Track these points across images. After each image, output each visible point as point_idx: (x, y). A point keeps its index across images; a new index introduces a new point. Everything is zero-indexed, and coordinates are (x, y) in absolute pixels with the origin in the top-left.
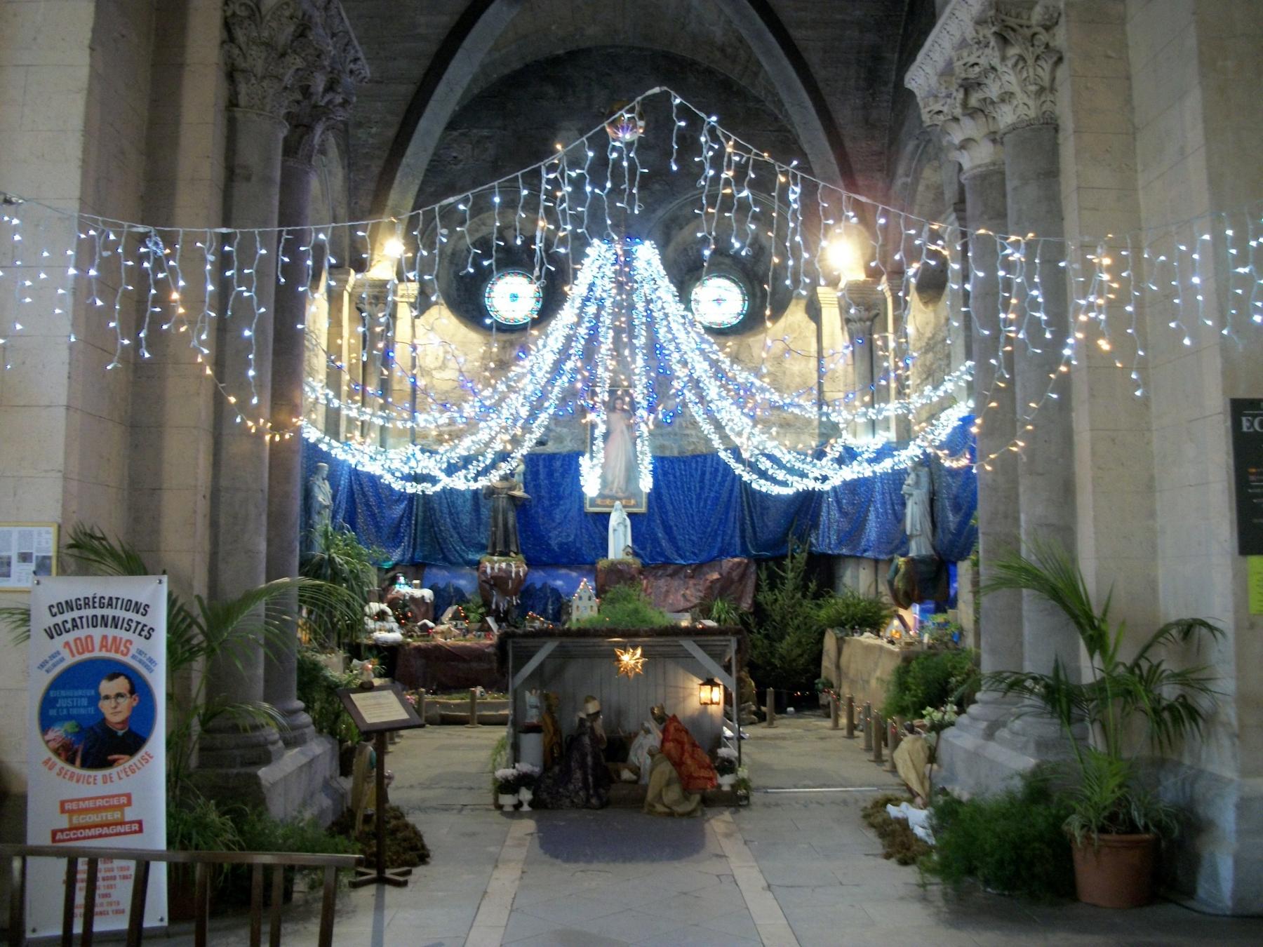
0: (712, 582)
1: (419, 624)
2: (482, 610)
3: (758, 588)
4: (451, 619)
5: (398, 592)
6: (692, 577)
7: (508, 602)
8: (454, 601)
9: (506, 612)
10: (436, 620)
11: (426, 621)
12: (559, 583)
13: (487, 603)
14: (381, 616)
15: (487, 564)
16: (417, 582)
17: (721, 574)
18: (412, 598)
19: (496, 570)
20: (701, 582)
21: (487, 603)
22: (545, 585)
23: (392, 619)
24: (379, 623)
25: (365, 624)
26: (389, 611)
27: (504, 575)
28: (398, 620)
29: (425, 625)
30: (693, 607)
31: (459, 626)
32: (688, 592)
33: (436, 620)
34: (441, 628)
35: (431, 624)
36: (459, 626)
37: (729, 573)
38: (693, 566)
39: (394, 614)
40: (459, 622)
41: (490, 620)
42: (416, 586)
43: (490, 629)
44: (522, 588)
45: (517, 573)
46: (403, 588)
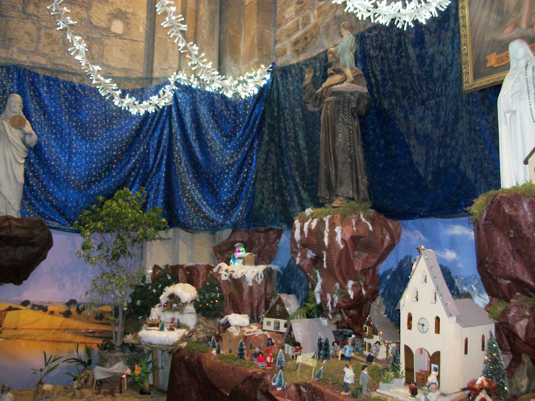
31: (283, 329)
40: (282, 322)
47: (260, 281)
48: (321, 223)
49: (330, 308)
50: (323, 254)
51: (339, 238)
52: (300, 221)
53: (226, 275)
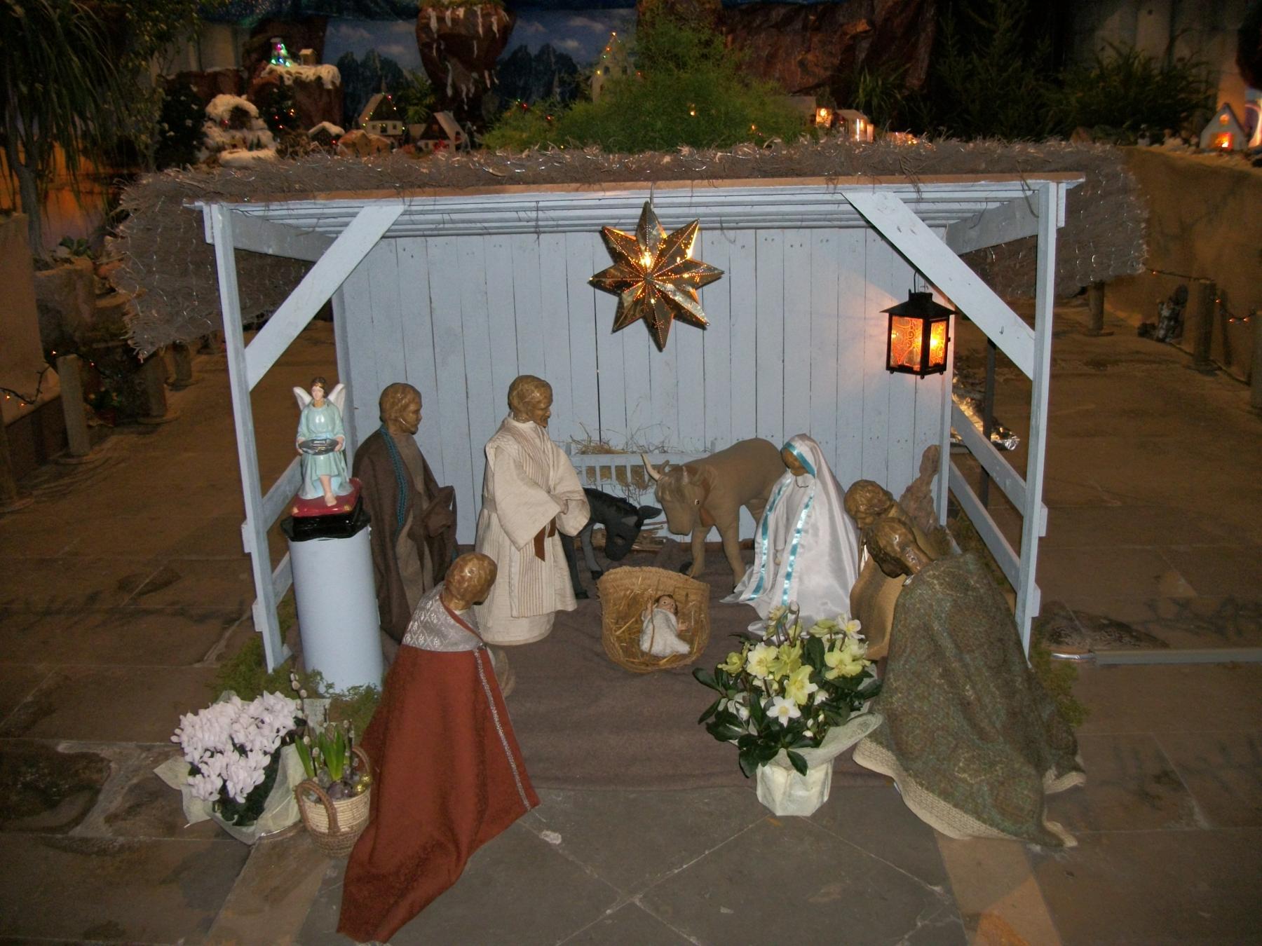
0: (854, 37)
1: (313, 130)
2: (430, 100)
3: (938, 50)
4: (372, 119)
5: (272, 71)
6: (817, 29)
7: (476, 81)
8: (383, 86)
9: (476, 101)
10: (348, 122)
11: (327, 124)
12: (571, 45)
13: (438, 86)
14: (238, 118)
15: (430, 10)
16: (307, 52)
17: (871, 23)
18: (299, 82)
19: (449, 23)
20: (835, 39)
21: (438, 86)
22: (546, 49)
23: (261, 122)
24: (238, 135)
25: (205, 135)
26: (252, 108)
27: (463, 31)
28: (272, 126)
29: (324, 130)
30: (818, 86)
31: (390, 131)
32: (810, 57)
33: (348, 122)
34: (356, 134)
35: (334, 129)
36: (390, 131)
37: (887, 20)
38: (820, 8)
39: (261, 115)
40: (390, 124)
41: (444, 120)
42: (306, 61)
43: (442, 135)
44: (505, 54)
45: (488, 28)
46: (284, 65)
47: (338, 82)
48: (470, 14)
49: (465, 100)
50: (473, 44)
51: (495, 28)
52: (434, 10)
53: (289, 79)
